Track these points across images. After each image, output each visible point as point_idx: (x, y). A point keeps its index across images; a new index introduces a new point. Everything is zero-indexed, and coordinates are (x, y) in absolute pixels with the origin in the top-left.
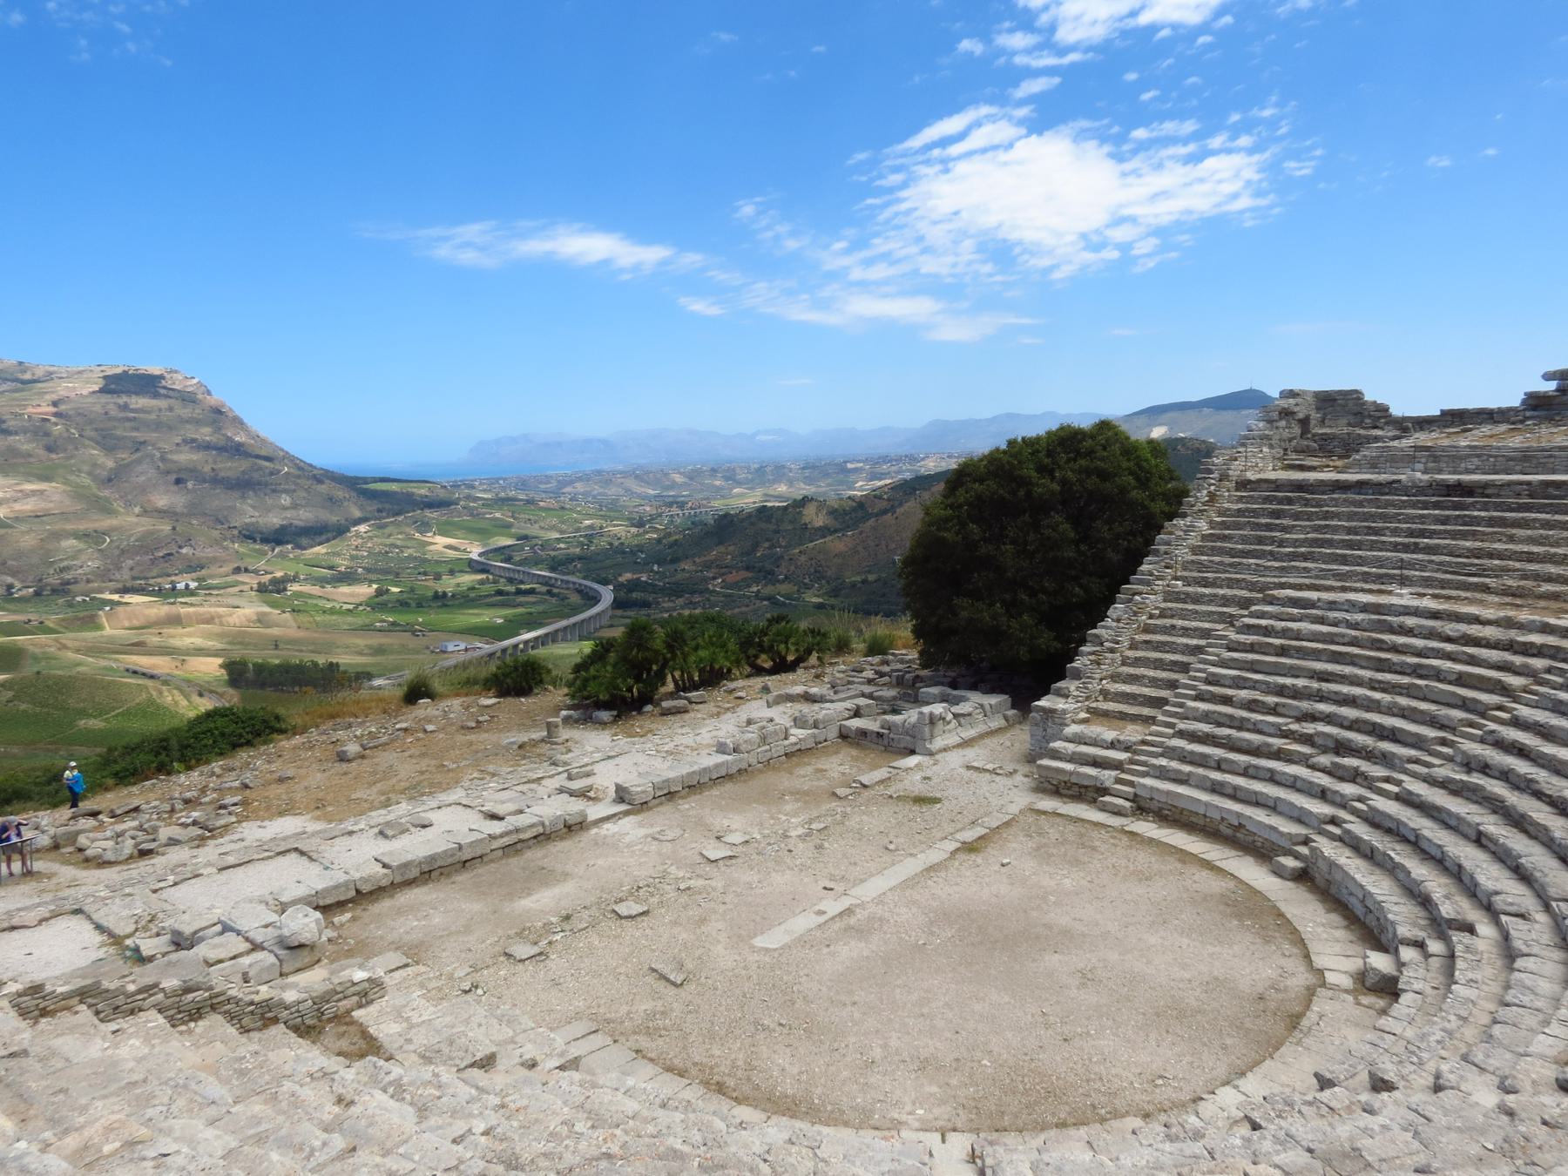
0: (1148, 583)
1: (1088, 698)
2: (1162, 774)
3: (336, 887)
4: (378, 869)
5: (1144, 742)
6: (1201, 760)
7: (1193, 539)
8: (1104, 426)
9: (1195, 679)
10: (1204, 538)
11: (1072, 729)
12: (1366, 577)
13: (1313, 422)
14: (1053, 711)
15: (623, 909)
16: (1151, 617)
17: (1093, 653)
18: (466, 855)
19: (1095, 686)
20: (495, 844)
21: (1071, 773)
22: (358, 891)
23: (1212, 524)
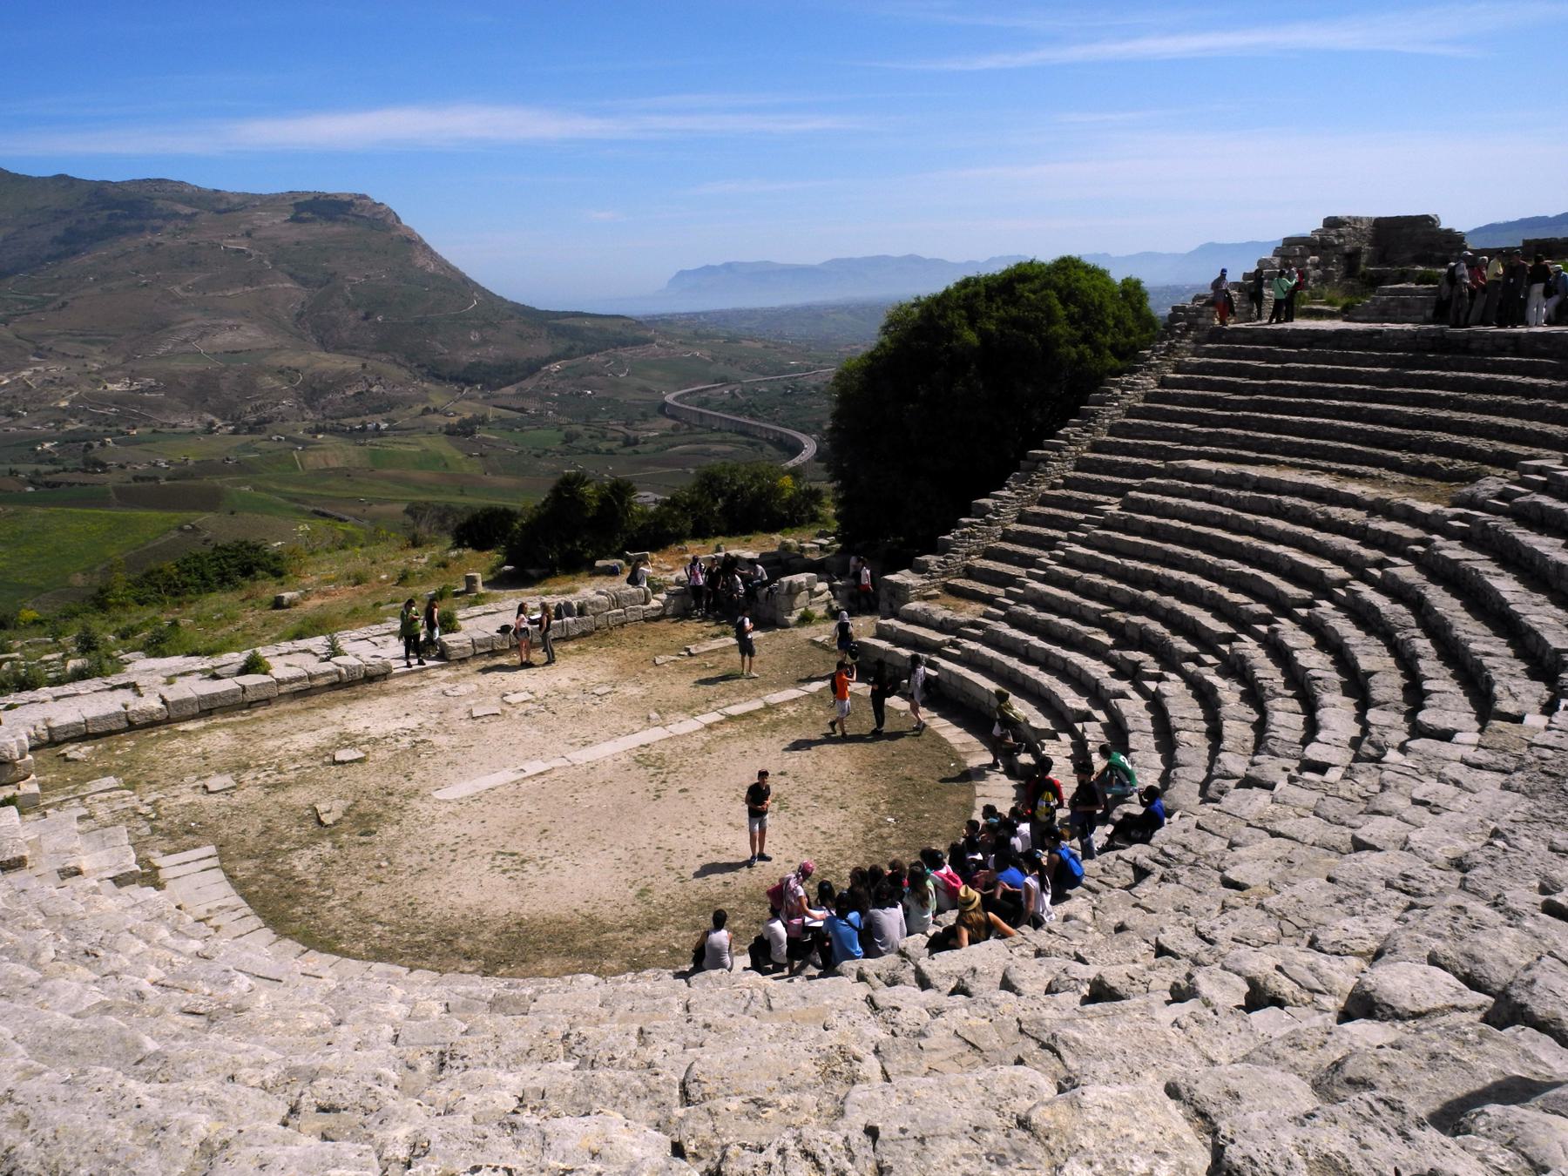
0: (1057, 448)
1: (945, 574)
2: (971, 661)
3: (106, 717)
4: (158, 705)
5: (974, 625)
6: (1010, 648)
7: (1134, 400)
9: (1053, 558)
10: (1149, 398)
11: (915, 605)
12: (1289, 449)
13: (1364, 259)
14: (897, 585)
15: (341, 755)
16: (1054, 486)
17: (970, 525)
18: (250, 697)
19: (957, 560)
20: (284, 689)
21: (887, 652)
22: (129, 722)
23: (1163, 383)
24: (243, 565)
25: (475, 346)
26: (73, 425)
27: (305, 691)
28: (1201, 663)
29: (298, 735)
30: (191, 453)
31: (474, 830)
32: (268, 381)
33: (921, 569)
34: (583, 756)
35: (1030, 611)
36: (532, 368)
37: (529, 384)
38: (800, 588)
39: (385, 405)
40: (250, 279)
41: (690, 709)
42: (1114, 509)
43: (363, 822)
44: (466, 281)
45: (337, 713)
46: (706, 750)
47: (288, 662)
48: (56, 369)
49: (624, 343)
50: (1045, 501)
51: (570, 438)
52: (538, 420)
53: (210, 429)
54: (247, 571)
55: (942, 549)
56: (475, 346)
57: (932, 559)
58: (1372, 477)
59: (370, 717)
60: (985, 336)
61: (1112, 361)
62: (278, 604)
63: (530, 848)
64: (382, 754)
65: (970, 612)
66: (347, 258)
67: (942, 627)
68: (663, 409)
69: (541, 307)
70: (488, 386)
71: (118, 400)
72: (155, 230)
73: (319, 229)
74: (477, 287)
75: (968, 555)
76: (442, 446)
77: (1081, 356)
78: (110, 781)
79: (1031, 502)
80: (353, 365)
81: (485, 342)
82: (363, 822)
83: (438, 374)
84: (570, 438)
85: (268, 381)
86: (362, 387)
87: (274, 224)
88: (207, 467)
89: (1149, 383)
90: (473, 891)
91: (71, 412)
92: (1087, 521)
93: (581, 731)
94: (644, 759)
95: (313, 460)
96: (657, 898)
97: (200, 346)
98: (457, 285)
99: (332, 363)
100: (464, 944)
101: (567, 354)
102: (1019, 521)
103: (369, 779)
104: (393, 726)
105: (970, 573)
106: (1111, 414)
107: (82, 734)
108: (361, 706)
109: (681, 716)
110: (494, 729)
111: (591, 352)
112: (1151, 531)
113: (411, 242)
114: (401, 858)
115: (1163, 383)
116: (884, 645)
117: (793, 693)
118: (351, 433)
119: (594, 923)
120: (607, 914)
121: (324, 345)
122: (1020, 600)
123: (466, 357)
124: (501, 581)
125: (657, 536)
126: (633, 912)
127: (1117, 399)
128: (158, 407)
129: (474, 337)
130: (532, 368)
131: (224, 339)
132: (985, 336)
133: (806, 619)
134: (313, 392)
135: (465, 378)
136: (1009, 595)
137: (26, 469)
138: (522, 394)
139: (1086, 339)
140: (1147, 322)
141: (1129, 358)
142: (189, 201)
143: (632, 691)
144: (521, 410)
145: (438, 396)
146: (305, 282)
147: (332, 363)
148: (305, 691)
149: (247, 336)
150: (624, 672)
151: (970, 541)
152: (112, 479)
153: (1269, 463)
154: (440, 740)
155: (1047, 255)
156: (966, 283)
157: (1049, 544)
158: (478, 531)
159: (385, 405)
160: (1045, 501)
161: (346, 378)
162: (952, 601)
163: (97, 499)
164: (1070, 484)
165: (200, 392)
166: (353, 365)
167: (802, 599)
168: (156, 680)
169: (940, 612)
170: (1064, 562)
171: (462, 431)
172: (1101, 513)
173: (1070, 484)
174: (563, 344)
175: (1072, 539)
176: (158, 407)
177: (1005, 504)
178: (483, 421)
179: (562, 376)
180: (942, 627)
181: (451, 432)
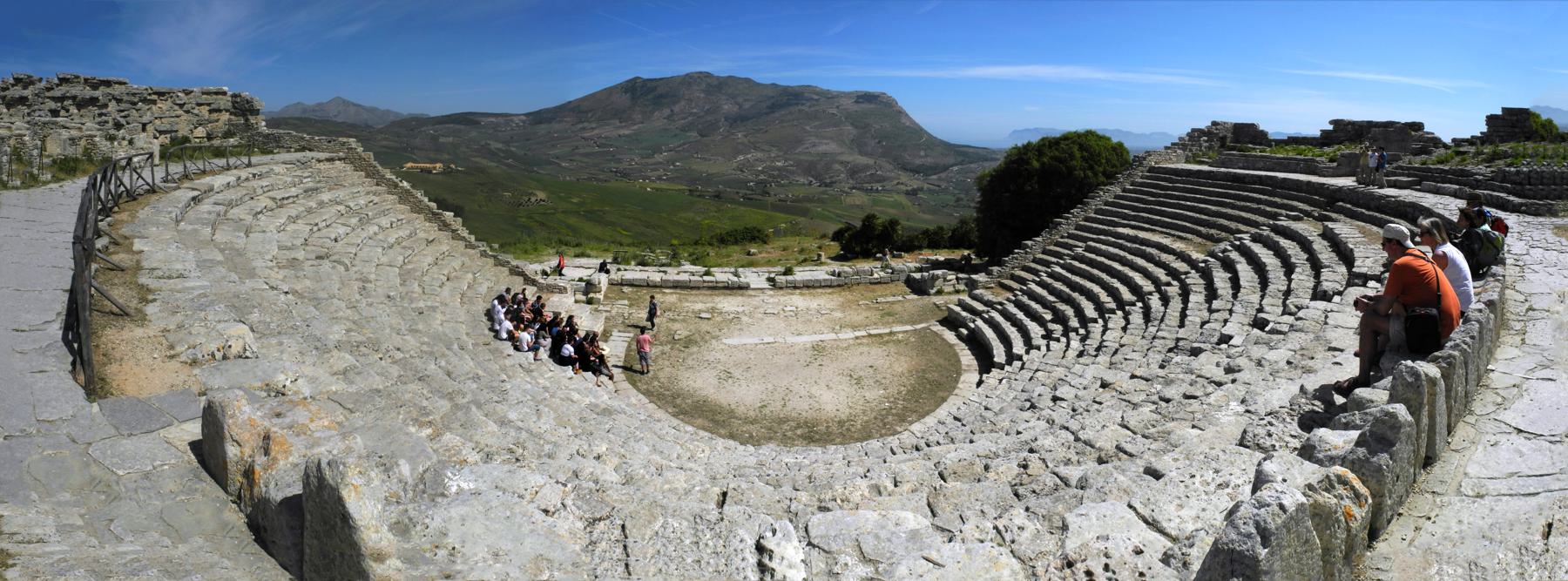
30: (801, 192)
32: (837, 166)
33: (989, 273)
36: (946, 168)
37: (943, 175)
39: (881, 180)
51: (958, 200)
52: (945, 191)
55: (1000, 264)
57: (995, 269)
65: (1003, 296)
66: (877, 119)
67: (986, 303)
70: (926, 175)
71: (779, 169)
73: (866, 106)
76: (903, 199)
80: (871, 162)
83: (905, 168)
84: (958, 200)
85: (837, 166)
87: (848, 104)
88: (807, 199)
95: (849, 200)
97: (812, 150)
98: (918, 131)
99: (862, 160)
101: (961, 163)
116: (958, 309)
118: (866, 191)
121: (861, 153)
123: (918, 162)
128: (793, 173)
130: (946, 168)
131: (822, 148)
133: (939, 292)
134: (854, 172)
135: (916, 171)
145: (904, 177)
147: (862, 160)
149: (831, 147)
151: (1015, 262)
152: (770, 200)
159: (881, 180)
161: (867, 167)
162: (999, 290)
163: (763, 206)
165: (809, 169)
166: (871, 162)
167: (939, 283)
169: (988, 296)
171: (912, 193)
174: (960, 159)
176: (793, 173)
178: (921, 189)
179: (958, 172)
180: (986, 303)
181: (907, 193)
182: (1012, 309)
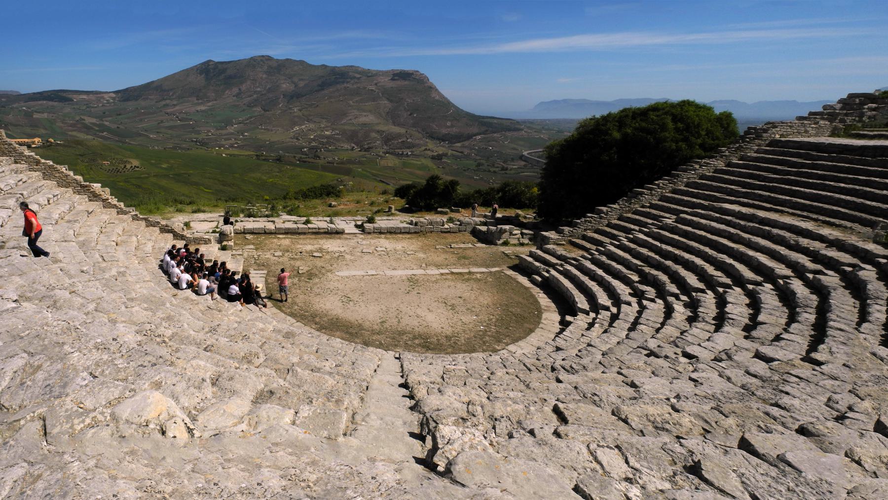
8: (685, 104)
16: (643, 207)
19: (579, 231)
21: (530, 263)
23: (729, 165)
24: (328, 192)
25: (449, 127)
26: (314, 144)
27: (318, 233)
28: (678, 298)
29: (308, 245)
30: (345, 156)
31: (341, 287)
32: (373, 135)
33: (560, 232)
34: (389, 273)
35: (604, 258)
36: (469, 137)
37: (466, 143)
38: (505, 231)
39: (410, 146)
40: (374, 100)
41: (438, 266)
42: (669, 221)
43: (310, 275)
44: (449, 103)
45: (322, 242)
46: (436, 282)
47: (318, 222)
48: (312, 126)
49: (510, 130)
50: (636, 212)
51: (479, 165)
52: (467, 157)
53: (352, 149)
54: (328, 194)
55: (570, 224)
56: (449, 127)
57: (566, 229)
58: (846, 227)
59: (332, 245)
60: (625, 136)
61: (700, 152)
62: (330, 206)
63: (355, 297)
64: (328, 257)
65: (576, 253)
66: (410, 95)
67: (559, 257)
68: (522, 157)
69: (477, 114)
70: (451, 142)
71: (328, 137)
72: (348, 82)
73: (400, 83)
74: (454, 106)
75: (585, 230)
76: (429, 163)
77: (679, 149)
78: (252, 247)
79: (629, 212)
80: (403, 131)
81: (452, 126)
82: (310, 275)
83: (432, 136)
84: (479, 165)
85: (373, 135)
86: (404, 139)
87: (385, 81)
88: (350, 162)
89: (720, 164)
90: (330, 305)
91: (314, 140)
92: (653, 224)
93: (394, 264)
94: (413, 281)
95: (383, 163)
96: (386, 325)
97: (354, 121)
98: (446, 104)
99: (396, 130)
100: (317, 319)
101: (484, 133)
102: (619, 219)
103: (319, 263)
104: (336, 249)
105: (584, 238)
106: (691, 176)
107: (252, 232)
108: (331, 241)
109: (434, 268)
110: (366, 257)
111: (495, 132)
112: (685, 234)
113: (432, 88)
114: (315, 289)
115: (729, 165)
116: (530, 259)
117: (484, 270)
118: (398, 155)
119: (360, 327)
120: (367, 325)
121: (394, 124)
122: (601, 253)
123: (444, 131)
124: (403, 210)
125: (466, 203)
126: (375, 327)
127: (695, 170)
128: (338, 140)
129: (449, 124)
130: (469, 137)
131: (363, 120)
132: (625, 136)
133: (506, 244)
134: (388, 139)
135: (442, 139)
136: (597, 250)
137: (298, 156)
138: (463, 147)
139: (685, 140)
140: (734, 134)
141: (711, 151)
142: (359, 73)
143: (421, 255)
144: (462, 152)
145: (431, 145)
146: (391, 101)
147: (396, 130)
148: (318, 233)
149: (370, 118)
150: (423, 249)
151: (588, 225)
152: (321, 162)
153: (777, 211)
154: (348, 257)
155: (676, 97)
156: (624, 110)
157: (627, 231)
158: (401, 192)
159: (410, 146)
160: (636, 212)
161: (399, 136)
162: (571, 248)
163: (314, 167)
164: (652, 206)
165: (352, 137)
166: (403, 131)
167: (505, 236)
168: (286, 221)
169: (560, 251)
170: (630, 240)
171: (438, 158)
172: (661, 221)
173: (652, 206)
174: (483, 129)
175: (641, 231)
176: (338, 140)
177: (612, 212)
178: (445, 155)
179: (481, 141)
180: (559, 257)
181: (433, 158)
182: (588, 264)
